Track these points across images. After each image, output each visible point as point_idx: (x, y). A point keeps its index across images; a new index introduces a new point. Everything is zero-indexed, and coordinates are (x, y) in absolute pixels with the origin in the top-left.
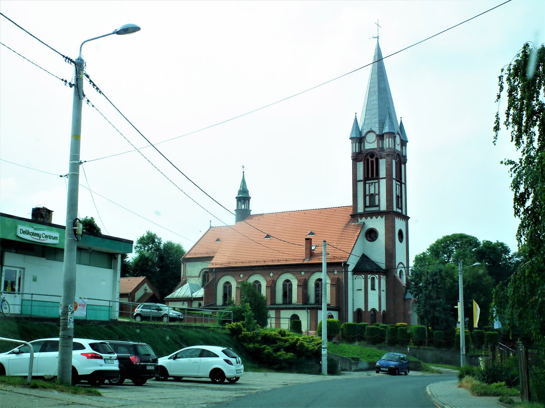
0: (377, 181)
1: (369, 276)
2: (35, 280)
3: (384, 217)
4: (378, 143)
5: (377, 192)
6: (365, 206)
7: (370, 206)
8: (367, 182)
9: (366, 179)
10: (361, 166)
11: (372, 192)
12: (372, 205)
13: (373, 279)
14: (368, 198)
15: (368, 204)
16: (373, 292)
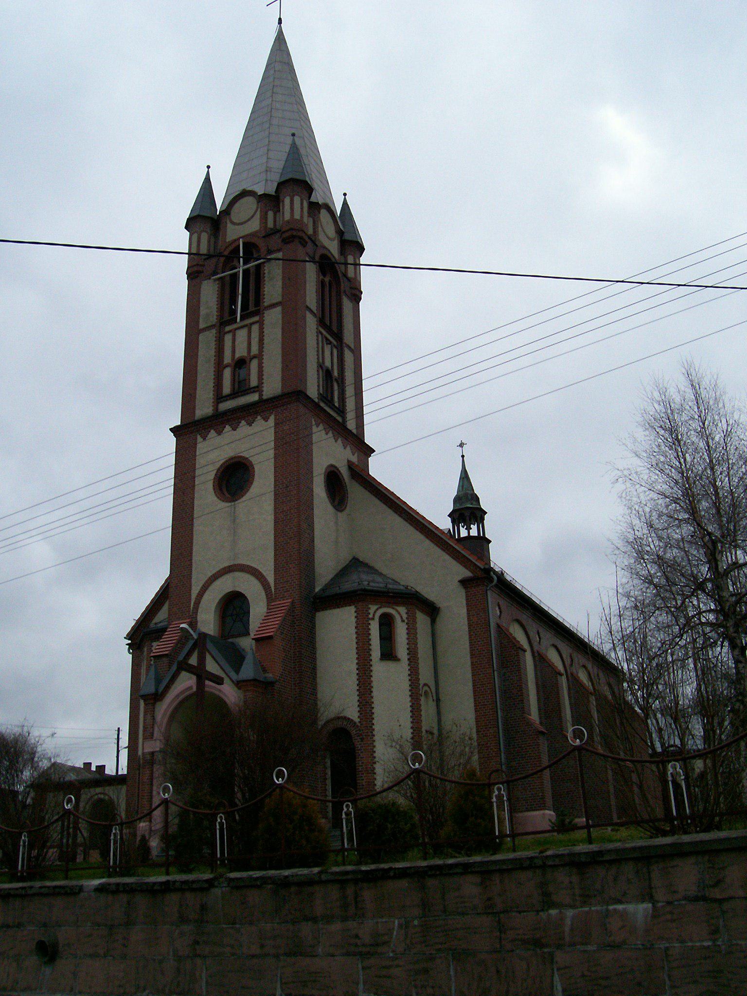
0: (256, 318)
1: (376, 611)
2: (48, 952)
3: (272, 418)
4: (264, 218)
5: (255, 350)
6: (219, 398)
7: (234, 395)
8: (227, 329)
9: (226, 319)
10: (210, 291)
11: (241, 352)
12: (241, 388)
13: (387, 623)
14: (227, 373)
15: (227, 389)
16: (391, 665)
